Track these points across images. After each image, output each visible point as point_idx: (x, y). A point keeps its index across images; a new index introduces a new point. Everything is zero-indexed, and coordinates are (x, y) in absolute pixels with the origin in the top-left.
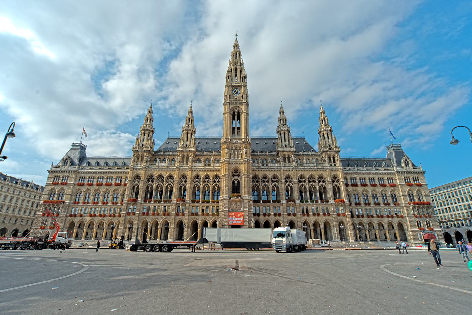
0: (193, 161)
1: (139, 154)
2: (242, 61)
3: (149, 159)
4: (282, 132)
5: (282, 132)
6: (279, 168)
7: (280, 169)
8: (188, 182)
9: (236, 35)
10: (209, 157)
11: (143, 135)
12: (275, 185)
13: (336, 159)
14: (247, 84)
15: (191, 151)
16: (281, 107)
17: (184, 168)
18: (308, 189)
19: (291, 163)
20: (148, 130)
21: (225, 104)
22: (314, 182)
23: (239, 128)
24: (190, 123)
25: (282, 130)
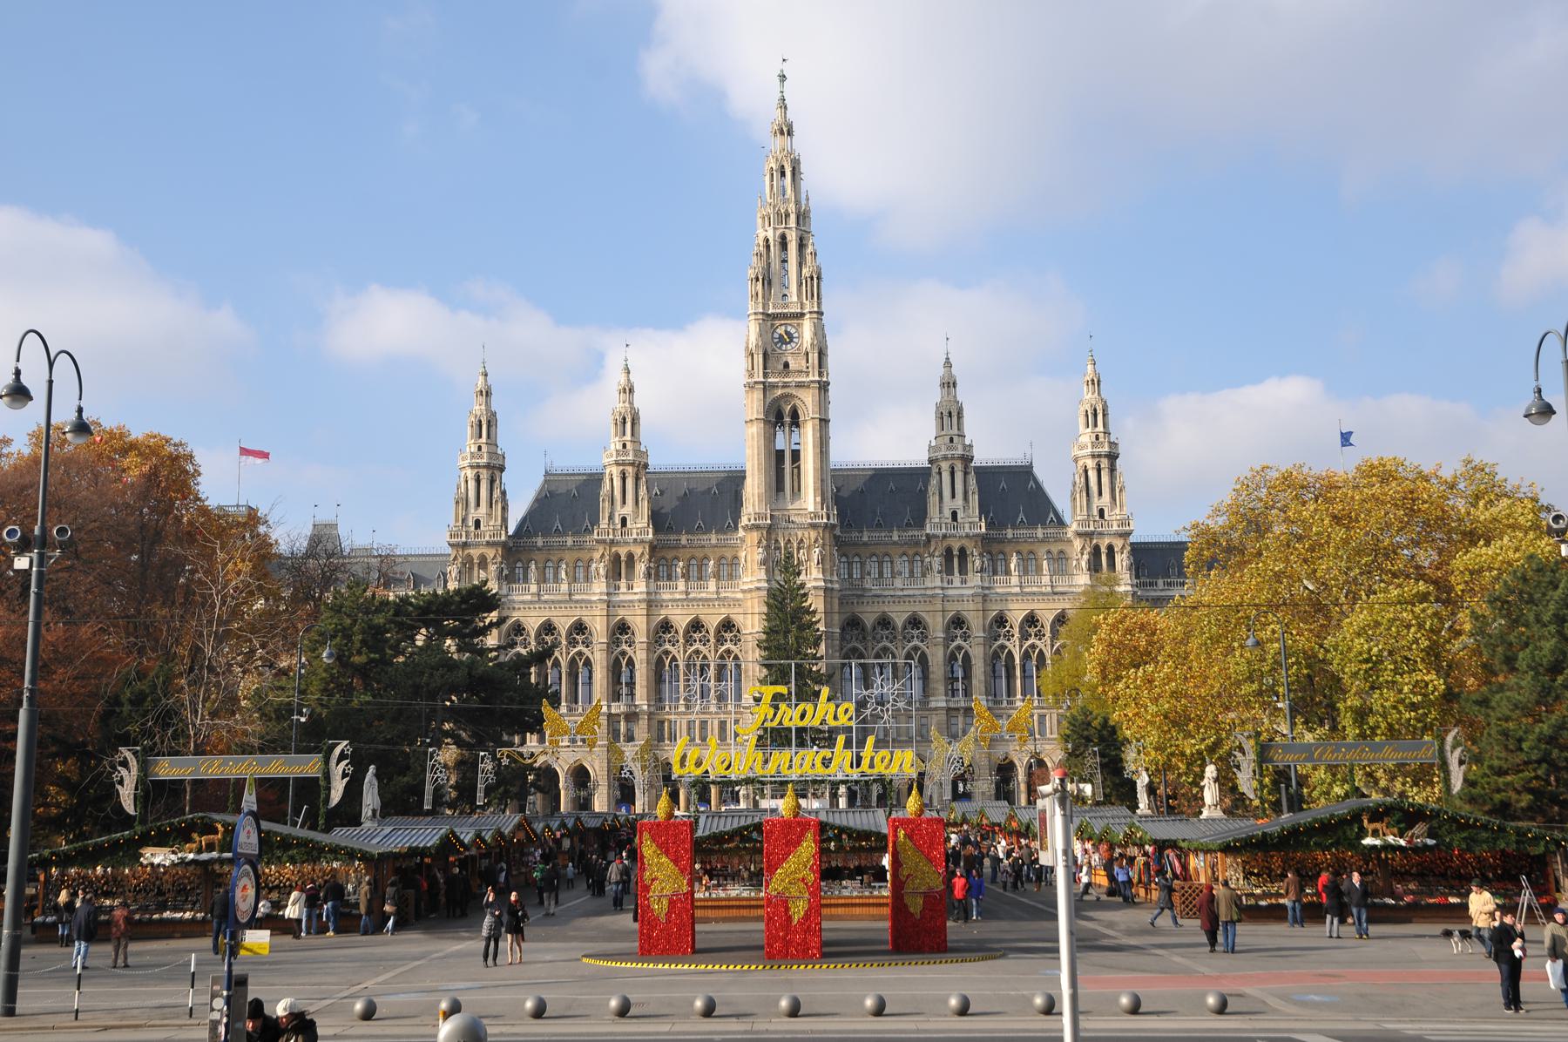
0: (648, 576)
1: (469, 555)
2: (803, 202)
3: (505, 572)
4: (945, 466)
5: (945, 466)
6: (929, 592)
7: (933, 596)
8: (638, 646)
9: (783, 78)
10: (699, 554)
11: (472, 485)
12: (916, 648)
13: (1118, 558)
14: (824, 309)
15: (642, 541)
16: (948, 364)
17: (622, 597)
18: (1017, 661)
19: (970, 574)
20: (488, 466)
21: (751, 387)
22: (1039, 635)
23: (796, 455)
24: (628, 437)
25: (945, 458)
